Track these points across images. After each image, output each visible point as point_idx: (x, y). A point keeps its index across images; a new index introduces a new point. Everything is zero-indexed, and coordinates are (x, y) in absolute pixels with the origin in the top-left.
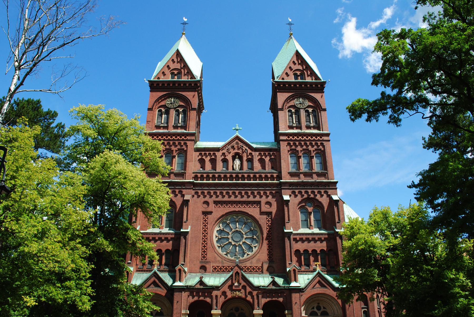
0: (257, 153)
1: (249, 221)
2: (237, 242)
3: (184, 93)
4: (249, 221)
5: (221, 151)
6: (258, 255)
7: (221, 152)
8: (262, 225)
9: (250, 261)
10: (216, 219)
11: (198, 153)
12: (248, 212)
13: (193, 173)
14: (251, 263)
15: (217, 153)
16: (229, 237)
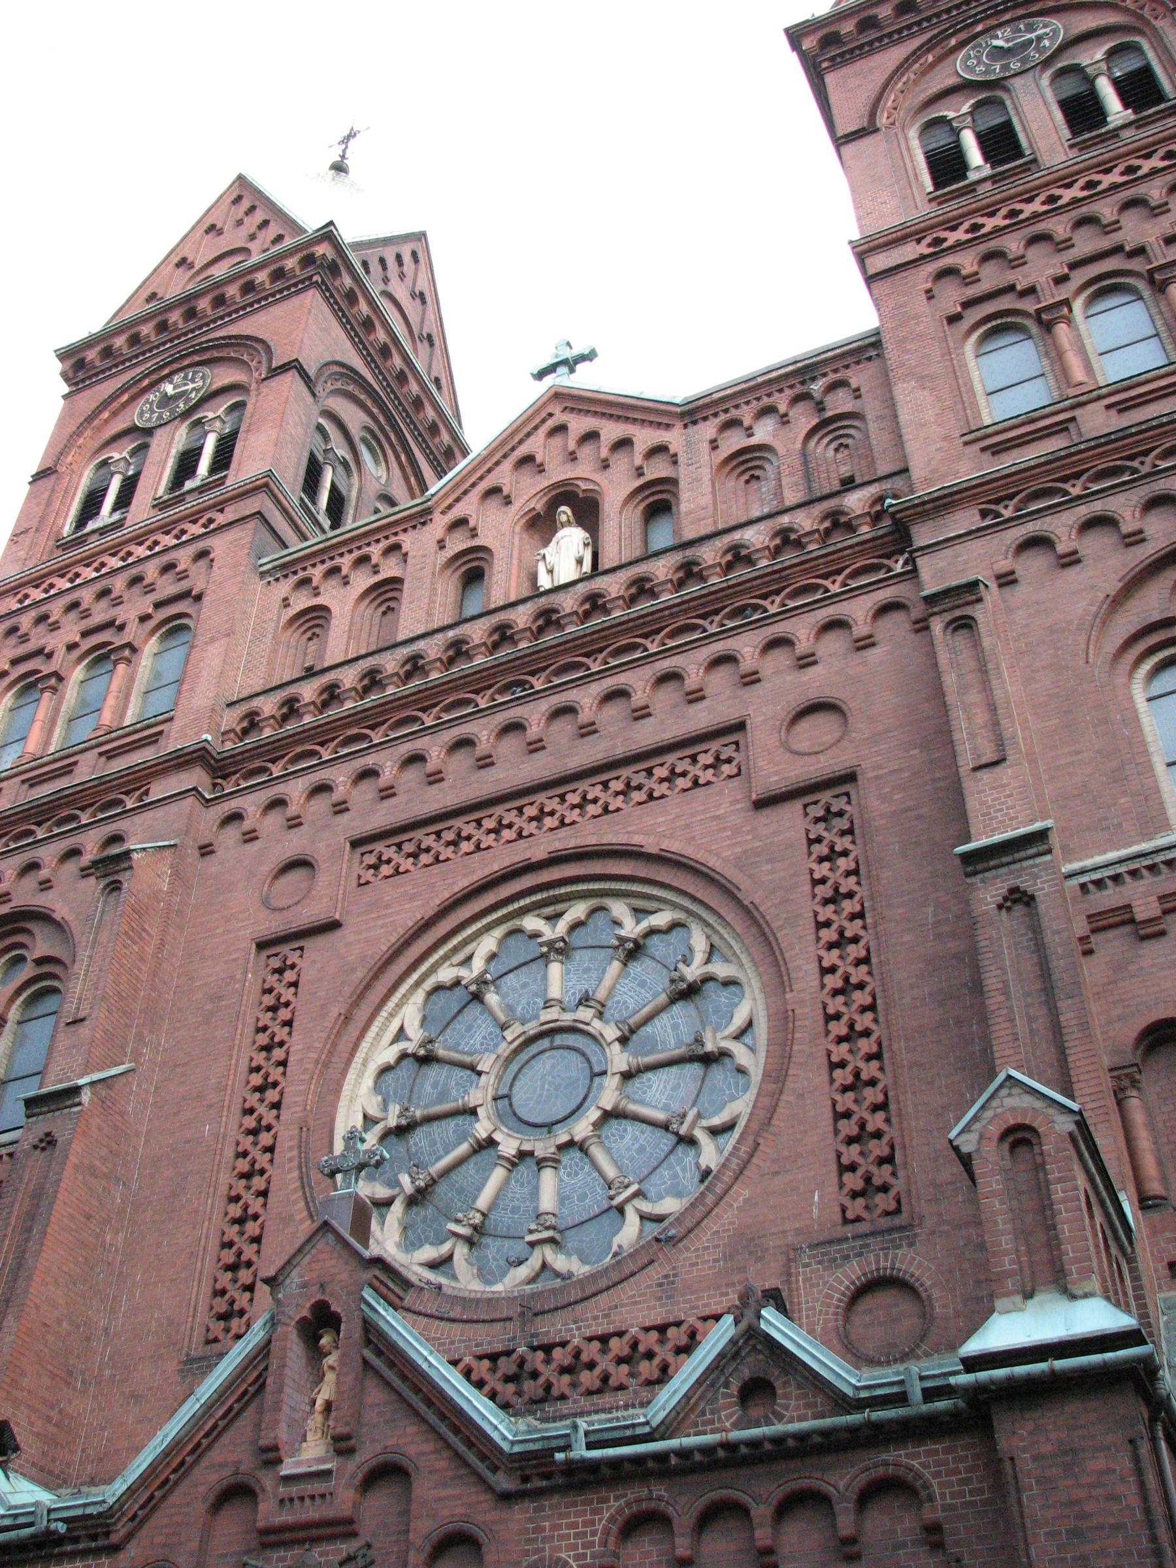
0: (708, 430)
1: (661, 919)
2: (549, 1127)
3: (233, 330)
4: (661, 919)
5: (436, 516)
6: (741, 1193)
7: (440, 522)
8: (768, 908)
9: (654, 1273)
10: (360, 974)
11: (284, 587)
12: (637, 839)
13: (230, 705)
14: (668, 1288)
15: (408, 541)
16: (479, 1094)
